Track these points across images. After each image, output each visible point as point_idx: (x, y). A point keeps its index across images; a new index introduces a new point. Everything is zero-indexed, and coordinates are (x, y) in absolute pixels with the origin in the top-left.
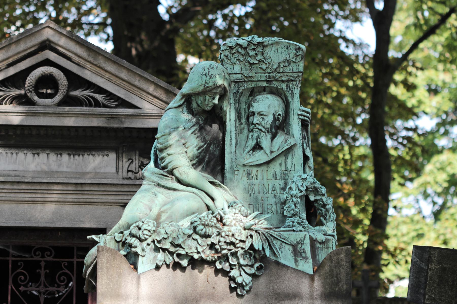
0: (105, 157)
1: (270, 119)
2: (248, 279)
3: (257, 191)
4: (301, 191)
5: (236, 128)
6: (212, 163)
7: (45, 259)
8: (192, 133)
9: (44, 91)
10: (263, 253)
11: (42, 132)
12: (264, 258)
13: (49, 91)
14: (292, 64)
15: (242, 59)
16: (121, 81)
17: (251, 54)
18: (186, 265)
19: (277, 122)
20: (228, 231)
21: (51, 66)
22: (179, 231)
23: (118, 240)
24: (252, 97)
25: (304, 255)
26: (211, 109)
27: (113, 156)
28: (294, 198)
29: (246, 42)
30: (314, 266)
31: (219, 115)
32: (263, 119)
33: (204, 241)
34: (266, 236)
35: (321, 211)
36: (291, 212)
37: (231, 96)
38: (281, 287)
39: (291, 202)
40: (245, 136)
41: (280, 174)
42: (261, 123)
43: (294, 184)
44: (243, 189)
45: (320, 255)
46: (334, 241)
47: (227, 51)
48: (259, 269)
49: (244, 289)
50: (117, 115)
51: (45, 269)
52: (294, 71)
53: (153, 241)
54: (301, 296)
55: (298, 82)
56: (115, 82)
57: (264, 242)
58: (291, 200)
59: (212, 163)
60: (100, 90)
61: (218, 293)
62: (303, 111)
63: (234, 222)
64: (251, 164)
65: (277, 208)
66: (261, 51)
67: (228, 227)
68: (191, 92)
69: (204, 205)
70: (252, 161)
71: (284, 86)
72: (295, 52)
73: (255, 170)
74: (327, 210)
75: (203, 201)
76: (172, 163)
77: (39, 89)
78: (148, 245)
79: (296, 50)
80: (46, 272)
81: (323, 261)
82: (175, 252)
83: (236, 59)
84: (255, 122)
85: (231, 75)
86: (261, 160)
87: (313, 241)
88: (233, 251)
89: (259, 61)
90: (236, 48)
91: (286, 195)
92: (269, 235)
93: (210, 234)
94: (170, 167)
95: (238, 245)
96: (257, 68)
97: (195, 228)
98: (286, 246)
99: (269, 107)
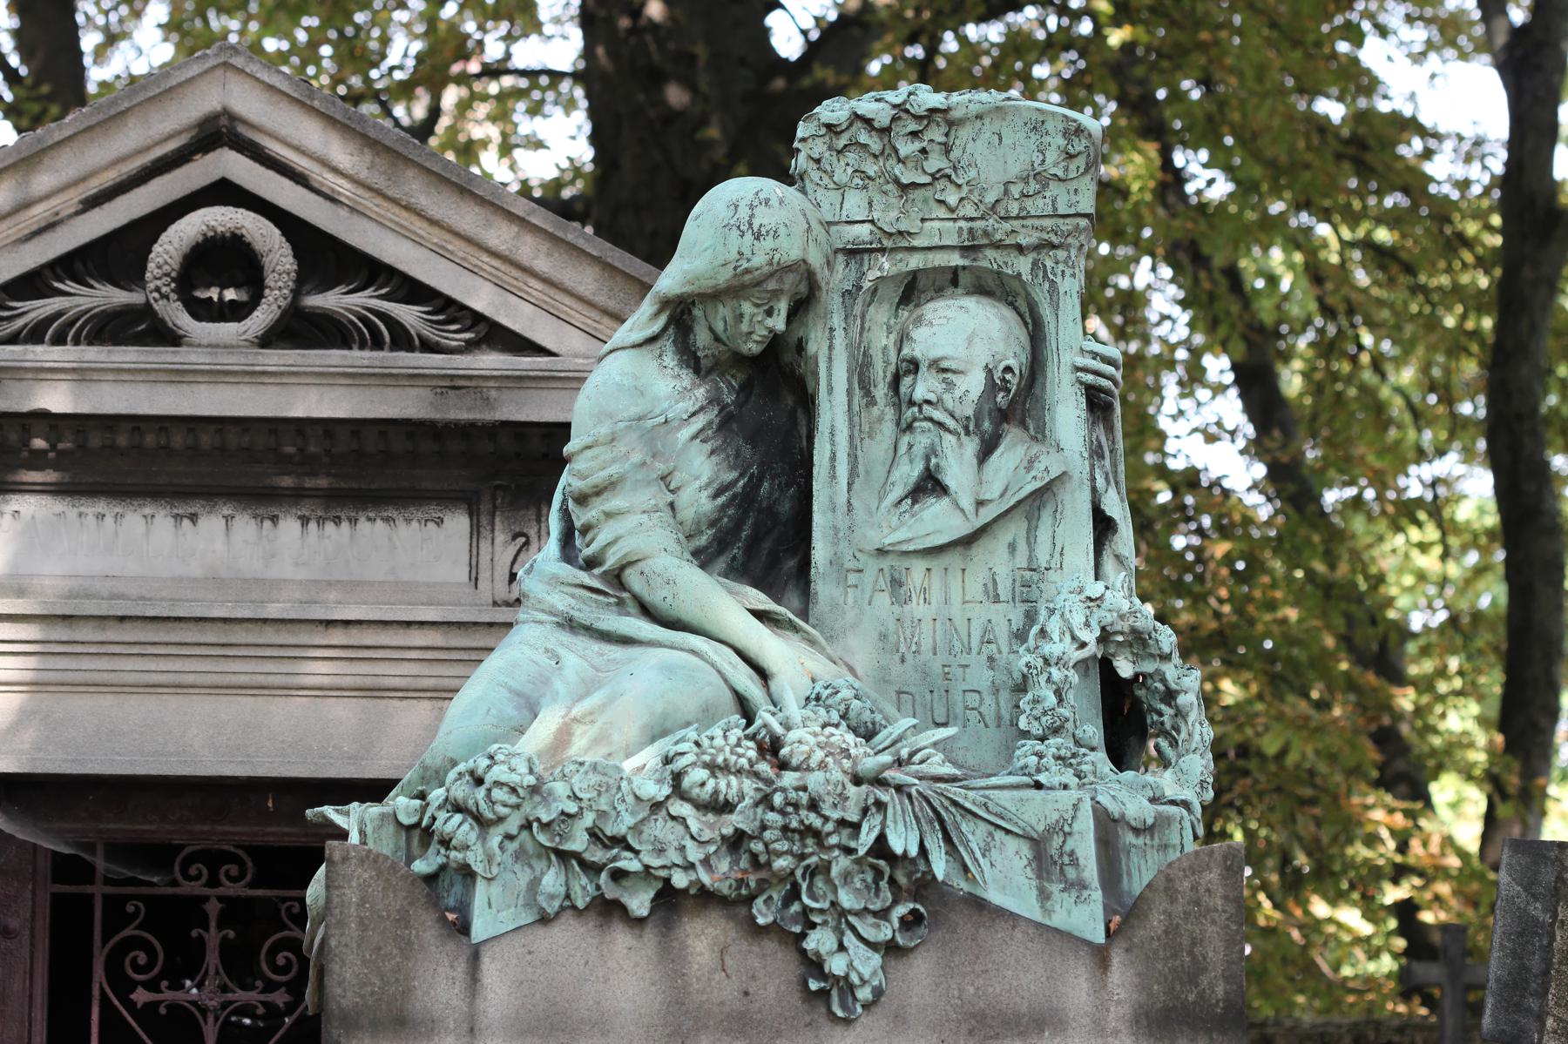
0: (431, 525)
1: (973, 384)
2: (867, 964)
3: (926, 644)
4: (1083, 645)
5: (851, 420)
6: (767, 545)
7: (221, 891)
8: (694, 437)
9: (214, 293)
10: (922, 867)
11: (206, 439)
12: (925, 886)
13: (230, 294)
14: (1054, 189)
15: (871, 169)
16: (485, 258)
17: (903, 152)
18: (645, 913)
19: (999, 399)
20: (797, 789)
21: (237, 204)
22: (619, 788)
23: (406, 821)
24: (911, 306)
25: (1071, 873)
26: (764, 351)
27: (458, 523)
28: (1054, 670)
29: (888, 107)
30: (1109, 911)
31: (793, 372)
32: (950, 385)
33: (711, 826)
34: (936, 804)
35: (1161, 714)
36: (1044, 719)
37: (832, 301)
38: (990, 990)
39: (1043, 683)
40: (885, 446)
41: (1009, 583)
42: (940, 400)
43: (1056, 617)
44: (876, 635)
45: (1135, 872)
46: (1187, 825)
47: (819, 141)
48: (911, 922)
49: (855, 998)
50: (470, 378)
51: (220, 927)
52: (1060, 212)
53: (527, 826)
54: (1061, 1021)
55: (1073, 252)
56: (464, 259)
57: (926, 827)
58: (1045, 675)
59: (767, 545)
60: (413, 290)
61: (760, 1011)
62: (1095, 355)
63: (819, 755)
64: (904, 547)
65: (998, 704)
66: (942, 139)
67: (797, 775)
68: (687, 289)
69: (728, 695)
70: (910, 535)
71: (1023, 265)
72: (1062, 142)
73: (918, 567)
74: (1180, 714)
75: (726, 681)
76: (621, 543)
77: (195, 288)
78: (509, 837)
79: (1065, 134)
80: (225, 938)
81: (1141, 896)
82: (605, 865)
83: (850, 170)
84: (920, 393)
85: (833, 229)
86: (940, 532)
87: (1108, 826)
88: (813, 860)
89: (932, 175)
90: (854, 129)
91: (1028, 658)
92: (947, 803)
93: (732, 795)
94: (611, 561)
95: (833, 840)
96: (925, 201)
97: (677, 777)
98: (1009, 839)
99: (970, 341)
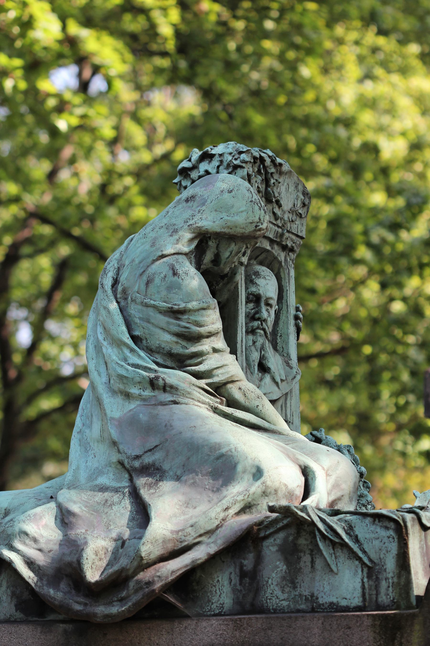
68: (226, 230)
